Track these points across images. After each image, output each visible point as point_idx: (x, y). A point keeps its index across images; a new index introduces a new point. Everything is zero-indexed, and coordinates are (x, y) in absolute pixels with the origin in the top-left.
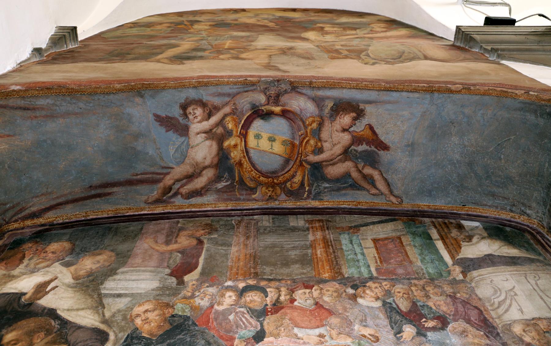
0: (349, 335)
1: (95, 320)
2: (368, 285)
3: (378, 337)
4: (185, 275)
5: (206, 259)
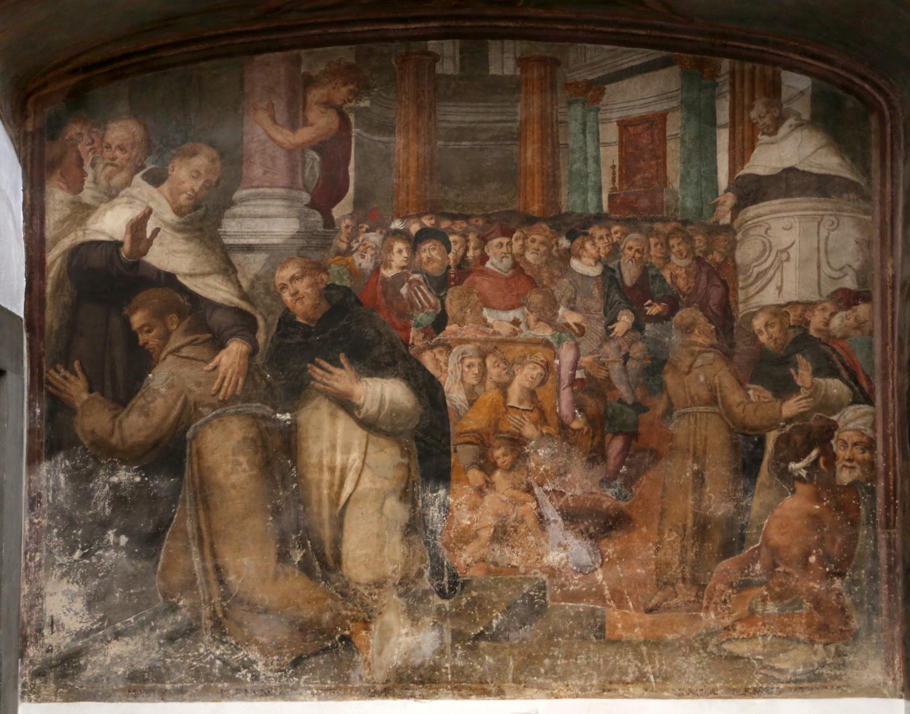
0: (550, 322)
1: (232, 295)
2: (590, 231)
3: (584, 328)
4: (333, 206)
5: (357, 168)
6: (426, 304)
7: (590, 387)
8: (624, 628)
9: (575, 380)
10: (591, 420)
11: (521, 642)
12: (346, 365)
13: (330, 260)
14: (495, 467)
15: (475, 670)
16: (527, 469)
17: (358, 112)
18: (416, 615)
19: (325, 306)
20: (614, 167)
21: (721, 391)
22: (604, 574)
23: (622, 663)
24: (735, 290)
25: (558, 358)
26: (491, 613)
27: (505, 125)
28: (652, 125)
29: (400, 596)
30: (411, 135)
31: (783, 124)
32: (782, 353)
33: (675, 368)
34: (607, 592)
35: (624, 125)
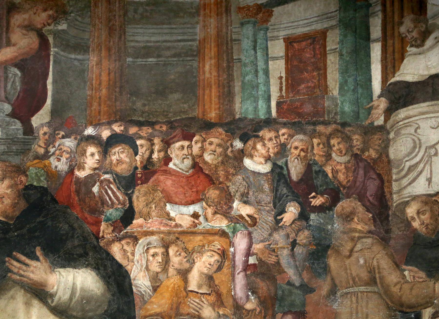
0: (226, 214)
2: (261, 134)
3: (256, 219)
4: (33, 116)
5: (55, 82)
6: (115, 201)
7: (262, 271)
9: (248, 265)
10: (262, 302)
12: (41, 258)
13: (29, 164)
17: (56, 34)
19: (23, 205)
20: (281, 78)
21: (379, 273)
24: (390, 182)
25: (233, 246)
27: (185, 43)
28: (314, 41)
30: (103, 54)
31: (429, 37)
32: (433, 237)
33: (338, 252)
35: (289, 42)
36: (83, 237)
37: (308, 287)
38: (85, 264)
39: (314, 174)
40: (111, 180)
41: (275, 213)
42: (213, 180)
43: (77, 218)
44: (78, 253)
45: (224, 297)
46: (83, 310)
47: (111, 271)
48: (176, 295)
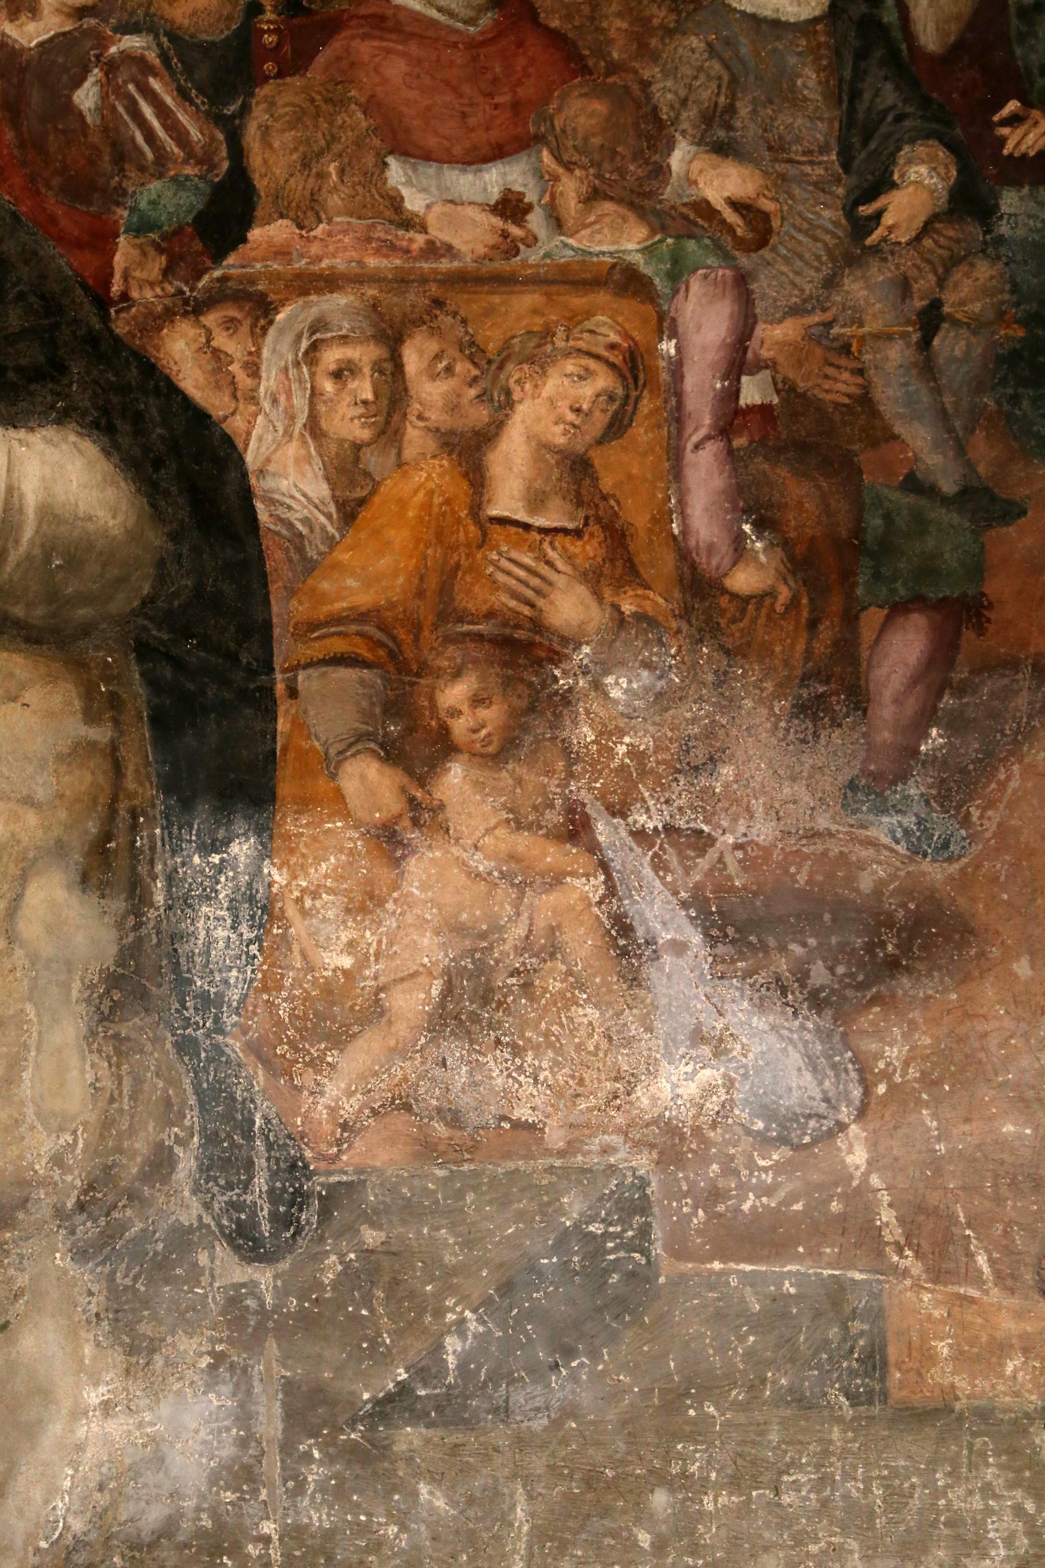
3: (766, 217)
7: (796, 436)
8: (958, 1356)
9: (738, 412)
10: (799, 562)
11: (556, 1424)
14: (445, 746)
15: (377, 1546)
16: (566, 750)
18: (145, 1328)
22: (873, 1145)
23: (963, 1500)
25: (674, 334)
26: (439, 1313)
29: (81, 1254)
34: (887, 1216)
36: (42, 297)
37: (994, 499)
38: (52, 407)
39: (1014, 21)
40: (153, 57)
41: (849, 192)
42: (582, 58)
43: (15, 216)
44: (23, 362)
45: (638, 545)
46: (52, 596)
47: (161, 437)
48: (439, 535)
